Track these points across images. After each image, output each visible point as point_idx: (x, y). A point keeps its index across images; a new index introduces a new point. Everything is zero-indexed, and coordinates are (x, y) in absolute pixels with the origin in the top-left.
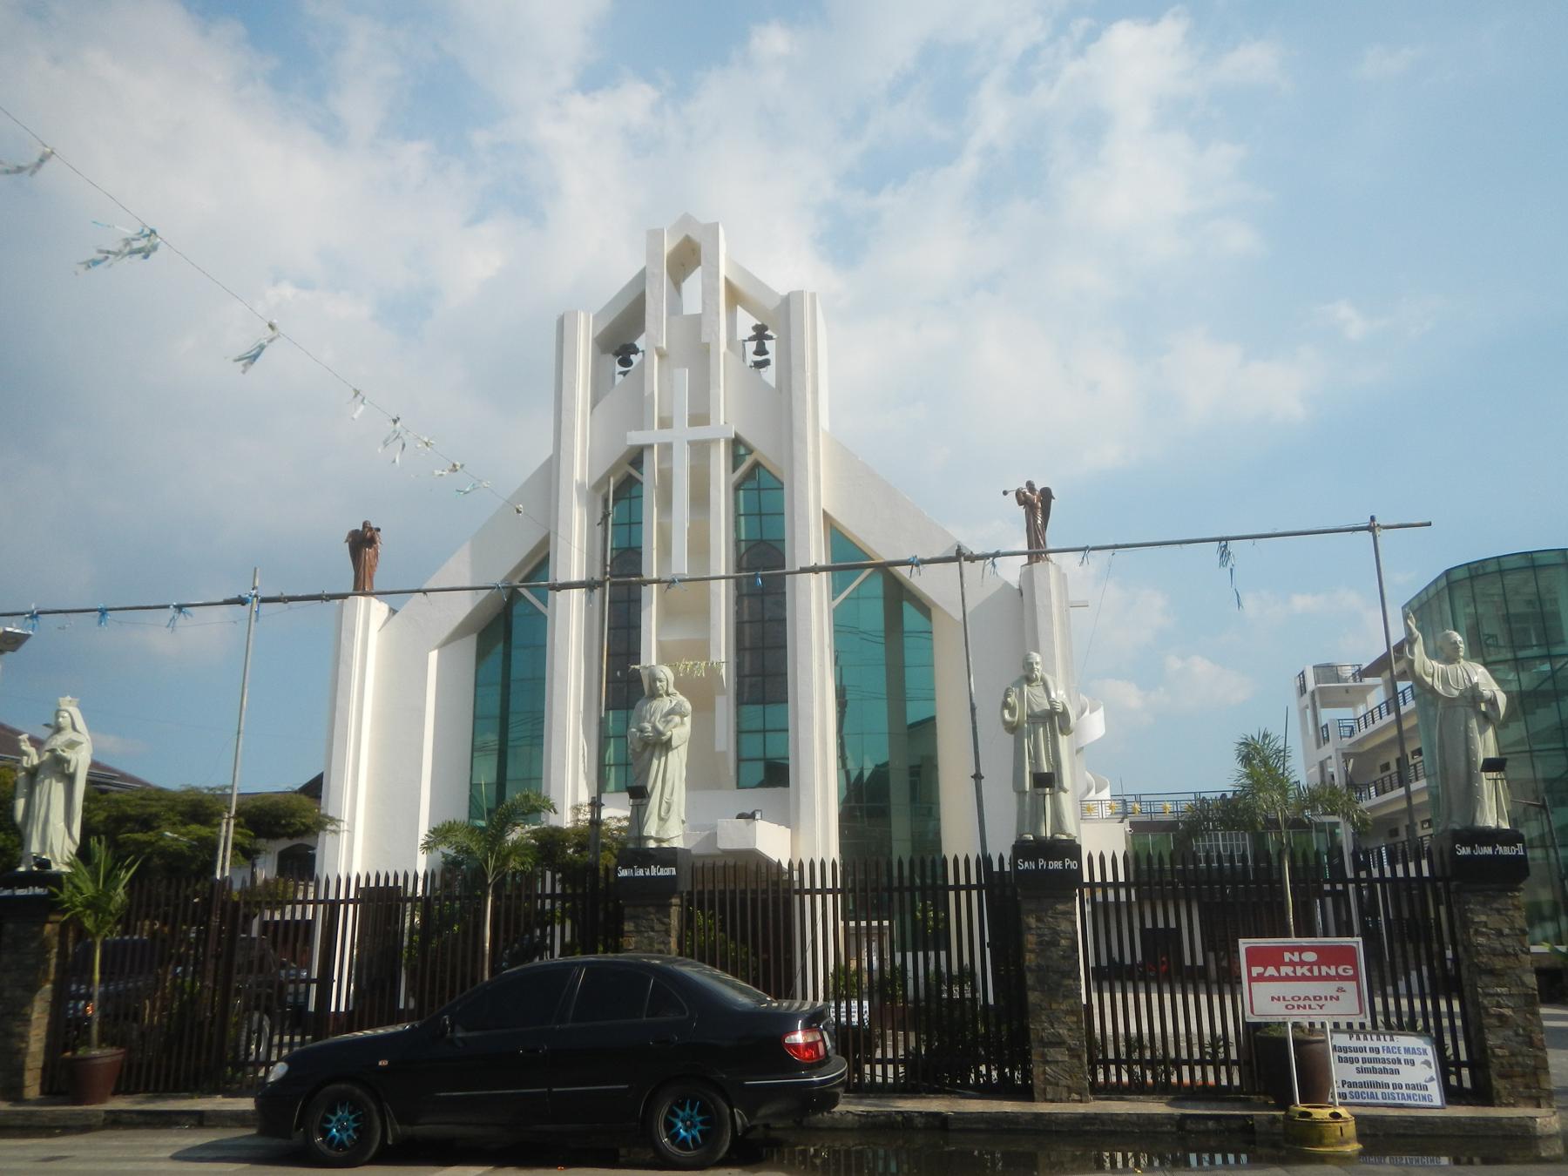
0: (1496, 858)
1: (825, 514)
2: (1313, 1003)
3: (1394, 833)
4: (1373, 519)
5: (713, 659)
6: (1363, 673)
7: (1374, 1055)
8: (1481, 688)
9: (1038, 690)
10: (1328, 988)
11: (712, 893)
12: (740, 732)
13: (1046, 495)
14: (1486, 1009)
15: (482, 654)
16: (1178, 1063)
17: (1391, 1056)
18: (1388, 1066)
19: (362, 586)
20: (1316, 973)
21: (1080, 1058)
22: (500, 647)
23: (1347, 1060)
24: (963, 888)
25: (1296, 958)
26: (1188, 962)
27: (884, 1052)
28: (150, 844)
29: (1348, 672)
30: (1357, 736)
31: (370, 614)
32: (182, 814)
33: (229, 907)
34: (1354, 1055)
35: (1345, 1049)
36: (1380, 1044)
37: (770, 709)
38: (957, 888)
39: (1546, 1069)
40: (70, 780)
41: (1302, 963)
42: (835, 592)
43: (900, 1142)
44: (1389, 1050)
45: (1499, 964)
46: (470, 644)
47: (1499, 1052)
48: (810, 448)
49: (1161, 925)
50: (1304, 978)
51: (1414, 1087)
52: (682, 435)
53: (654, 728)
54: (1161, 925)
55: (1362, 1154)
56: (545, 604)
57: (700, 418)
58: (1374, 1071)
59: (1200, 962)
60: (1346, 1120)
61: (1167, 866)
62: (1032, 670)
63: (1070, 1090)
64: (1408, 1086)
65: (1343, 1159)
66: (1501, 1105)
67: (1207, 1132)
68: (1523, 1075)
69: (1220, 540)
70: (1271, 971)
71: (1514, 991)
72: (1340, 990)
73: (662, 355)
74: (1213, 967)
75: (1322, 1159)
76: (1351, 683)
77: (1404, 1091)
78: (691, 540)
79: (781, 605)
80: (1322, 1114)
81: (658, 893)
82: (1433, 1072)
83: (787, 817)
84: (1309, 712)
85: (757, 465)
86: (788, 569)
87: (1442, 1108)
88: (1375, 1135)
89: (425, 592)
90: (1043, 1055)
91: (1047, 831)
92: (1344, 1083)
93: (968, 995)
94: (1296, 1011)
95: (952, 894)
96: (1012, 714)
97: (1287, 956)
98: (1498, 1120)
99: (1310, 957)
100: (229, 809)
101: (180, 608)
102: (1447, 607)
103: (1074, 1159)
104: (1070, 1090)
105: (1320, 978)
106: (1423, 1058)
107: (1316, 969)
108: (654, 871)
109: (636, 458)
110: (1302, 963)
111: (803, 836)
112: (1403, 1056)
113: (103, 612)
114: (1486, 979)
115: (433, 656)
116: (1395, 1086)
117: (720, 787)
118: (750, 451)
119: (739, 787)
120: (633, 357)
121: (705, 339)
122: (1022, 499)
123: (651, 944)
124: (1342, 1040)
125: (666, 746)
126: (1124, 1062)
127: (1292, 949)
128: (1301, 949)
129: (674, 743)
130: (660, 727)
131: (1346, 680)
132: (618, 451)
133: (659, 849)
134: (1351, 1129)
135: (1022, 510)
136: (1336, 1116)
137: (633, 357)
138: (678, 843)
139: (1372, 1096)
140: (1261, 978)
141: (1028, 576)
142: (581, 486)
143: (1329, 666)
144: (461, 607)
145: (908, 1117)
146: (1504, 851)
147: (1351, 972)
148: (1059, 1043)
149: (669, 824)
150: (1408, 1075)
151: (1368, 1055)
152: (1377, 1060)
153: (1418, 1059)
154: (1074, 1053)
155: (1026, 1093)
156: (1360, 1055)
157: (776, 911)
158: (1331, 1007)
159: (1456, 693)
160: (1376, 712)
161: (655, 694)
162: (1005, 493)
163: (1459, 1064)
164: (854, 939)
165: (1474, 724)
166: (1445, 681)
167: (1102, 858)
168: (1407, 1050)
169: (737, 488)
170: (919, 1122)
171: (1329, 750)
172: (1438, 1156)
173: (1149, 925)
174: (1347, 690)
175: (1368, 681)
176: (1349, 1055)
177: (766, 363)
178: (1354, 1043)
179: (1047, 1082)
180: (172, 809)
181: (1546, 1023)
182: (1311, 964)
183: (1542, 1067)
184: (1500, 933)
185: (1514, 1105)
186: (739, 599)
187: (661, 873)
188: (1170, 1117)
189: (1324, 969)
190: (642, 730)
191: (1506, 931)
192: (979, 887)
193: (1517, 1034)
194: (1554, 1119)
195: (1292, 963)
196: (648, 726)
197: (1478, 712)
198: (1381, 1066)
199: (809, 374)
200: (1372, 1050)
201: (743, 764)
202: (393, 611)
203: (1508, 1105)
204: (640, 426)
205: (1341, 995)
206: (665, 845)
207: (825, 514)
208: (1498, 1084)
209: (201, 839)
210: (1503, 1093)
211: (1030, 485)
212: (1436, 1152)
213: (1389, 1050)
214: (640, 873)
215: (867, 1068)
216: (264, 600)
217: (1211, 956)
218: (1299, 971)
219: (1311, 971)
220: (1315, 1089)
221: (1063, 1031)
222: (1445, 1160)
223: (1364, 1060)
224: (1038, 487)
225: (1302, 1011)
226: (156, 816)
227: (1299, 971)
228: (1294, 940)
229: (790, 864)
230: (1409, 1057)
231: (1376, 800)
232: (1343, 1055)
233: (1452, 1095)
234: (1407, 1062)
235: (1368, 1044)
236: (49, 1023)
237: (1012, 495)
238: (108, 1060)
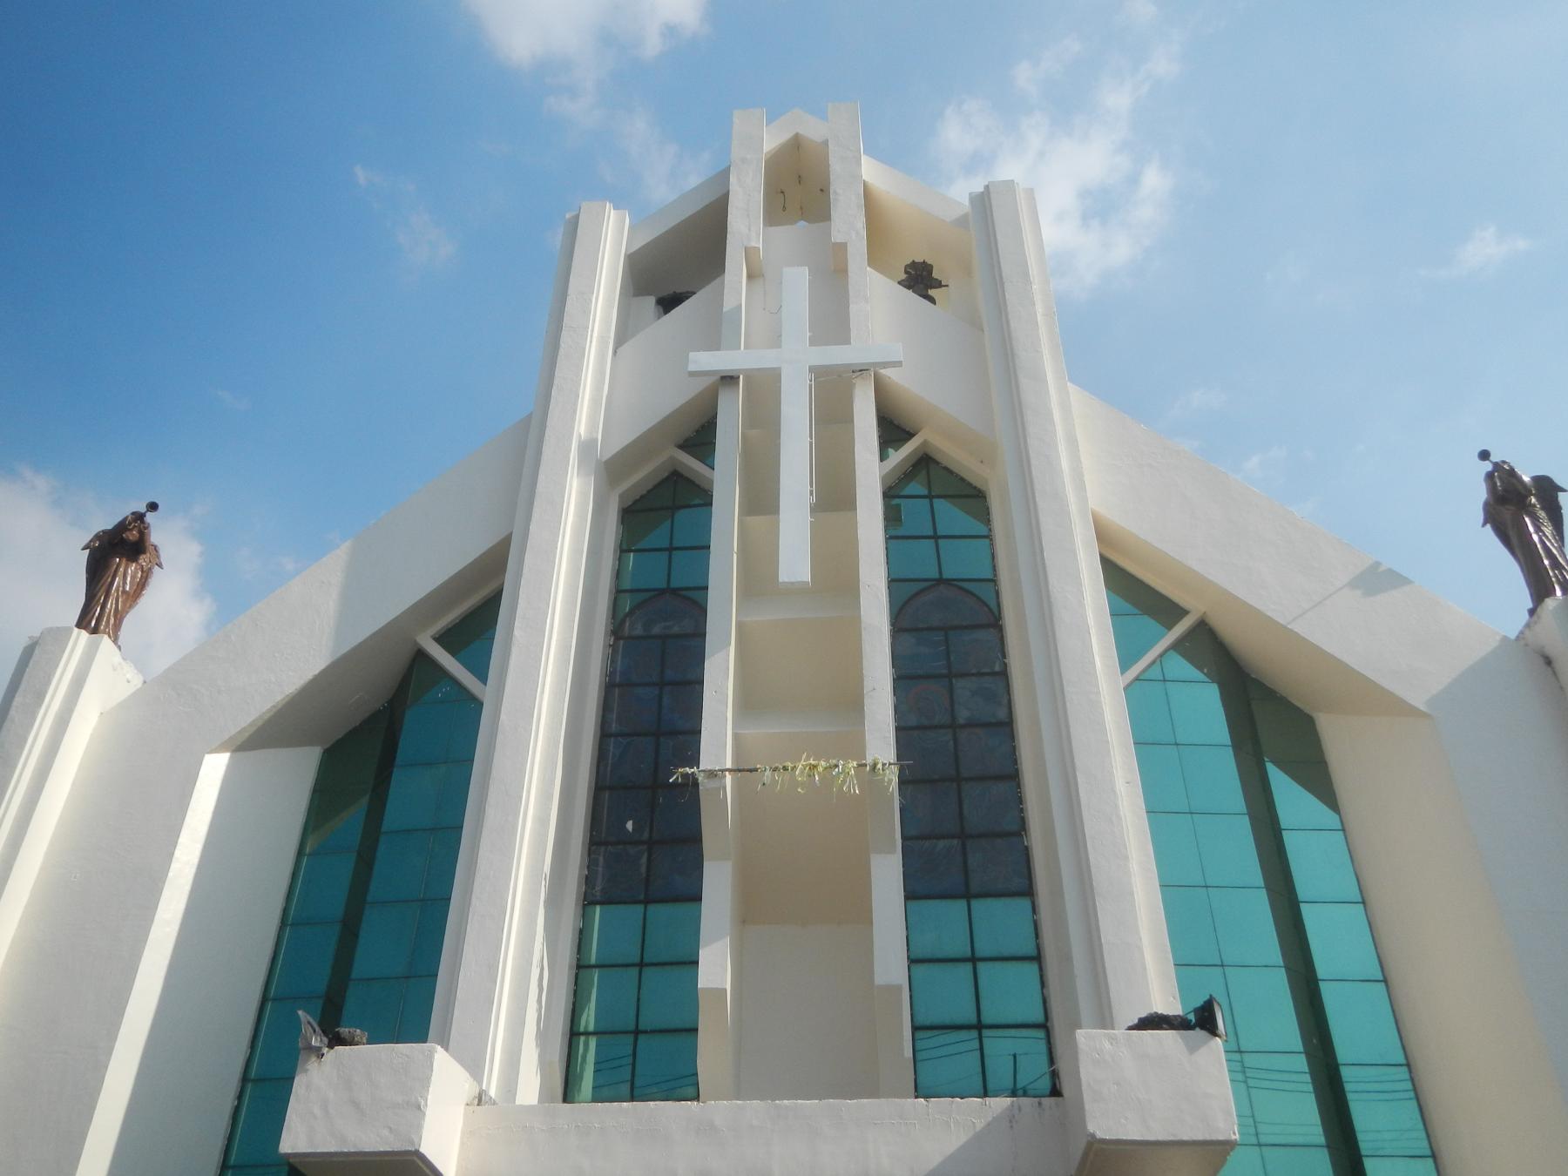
15: (326, 799)
22: (364, 802)
56: (483, 678)
78: (802, 561)
115: (214, 767)
117: (871, 1090)
132: (672, 398)
142: (587, 447)
237: (1488, 466)
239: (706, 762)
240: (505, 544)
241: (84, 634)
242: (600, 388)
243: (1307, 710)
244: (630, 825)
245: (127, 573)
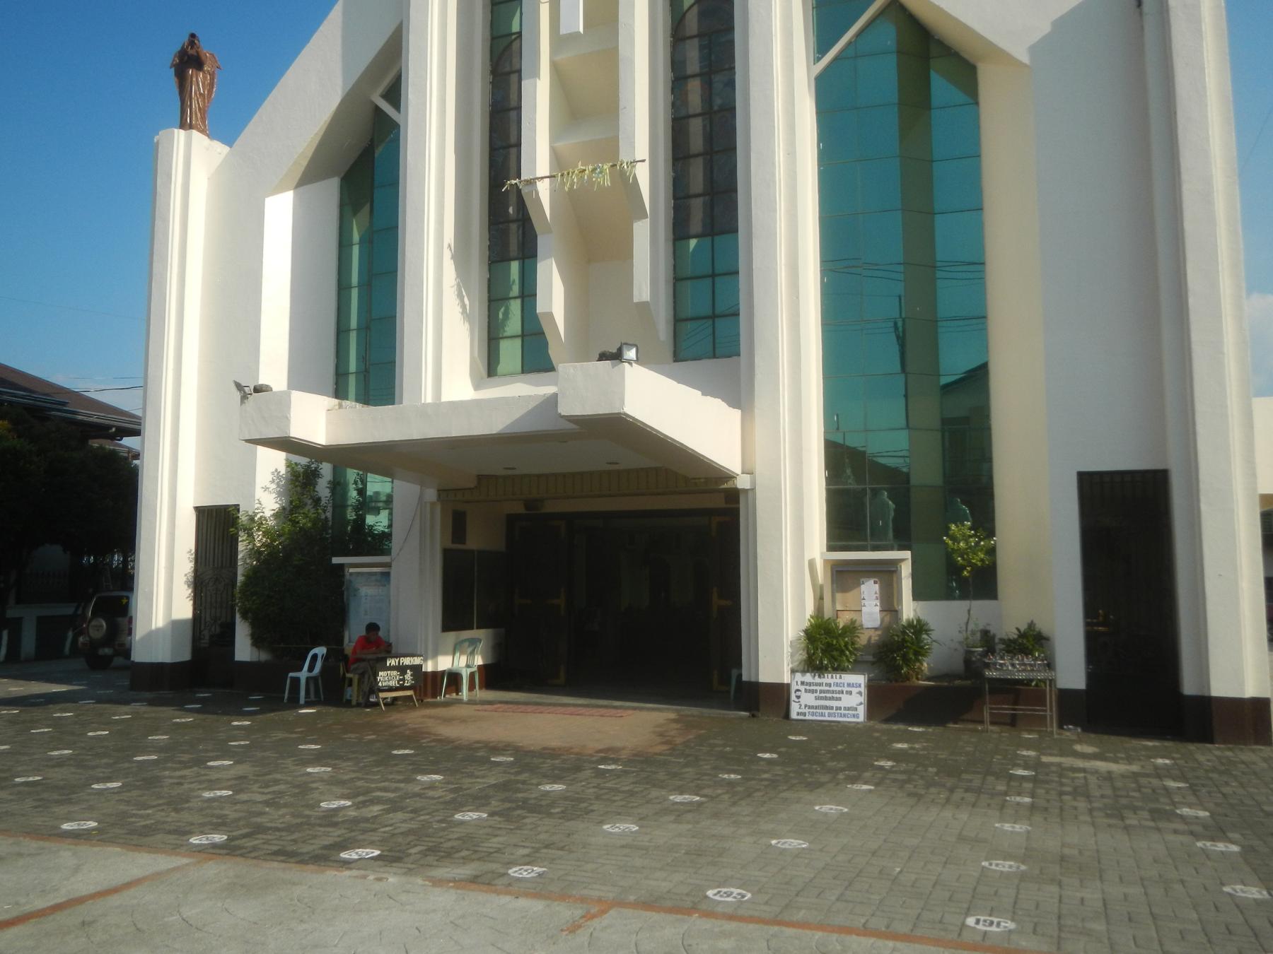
5: (624, 157)
12: (679, 279)
37: (717, 238)
46: (330, 189)
83: (738, 393)
164: (844, 576)
239: (525, 175)
241: (182, 132)
243: (972, 61)
244: (511, 210)
245: (198, 81)
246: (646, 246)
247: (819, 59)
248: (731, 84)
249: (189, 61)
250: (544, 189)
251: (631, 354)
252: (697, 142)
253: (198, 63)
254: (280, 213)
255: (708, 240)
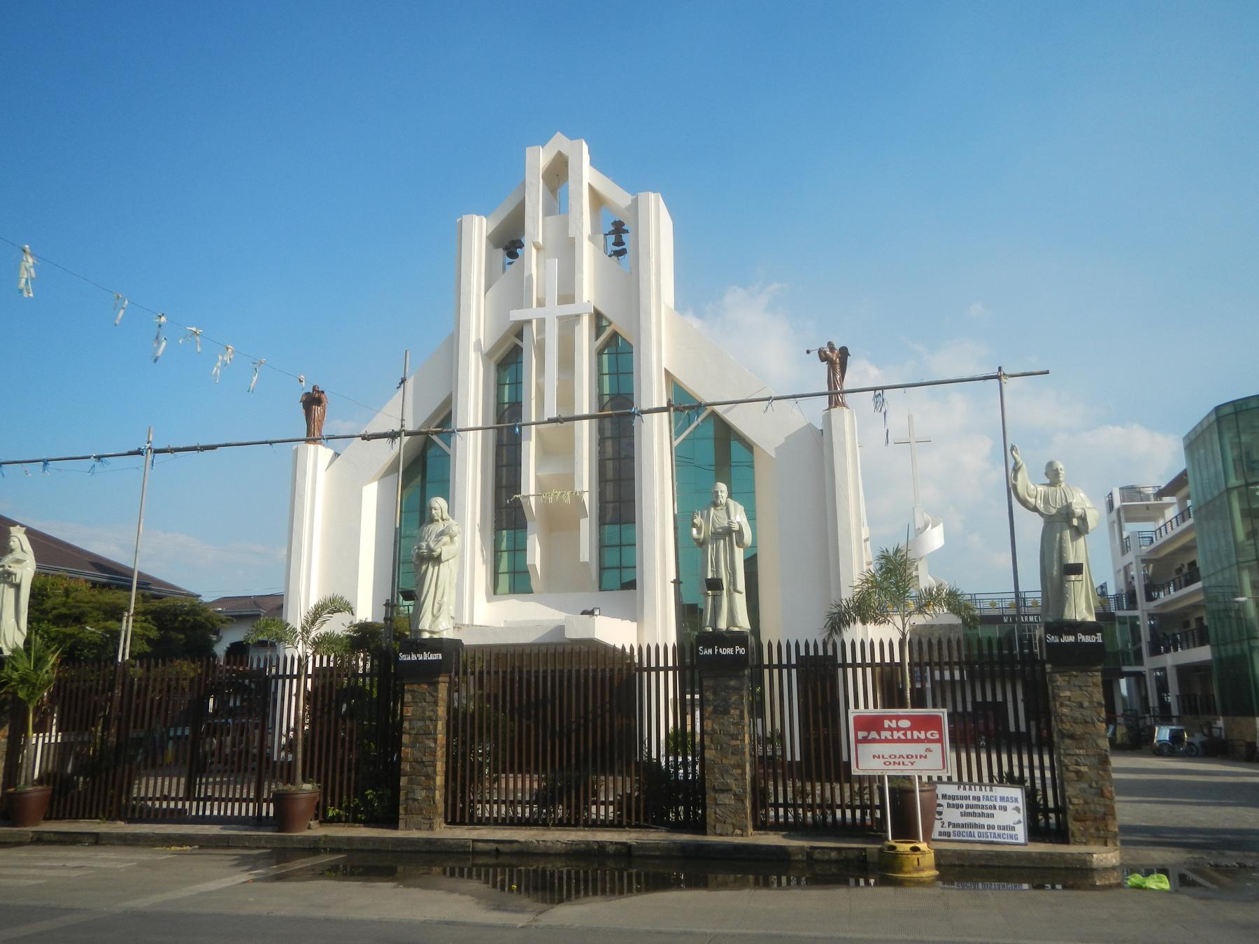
0: (1077, 645)
1: (666, 371)
2: (906, 761)
3: (1187, 624)
4: (1000, 369)
5: (577, 489)
6: (1161, 494)
7: (976, 802)
8: (1074, 506)
9: (722, 513)
10: (919, 749)
11: (562, 672)
12: (602, 546)
13: (844, 353)
14: (1067, 766)
16: (832, 807)
17: (989, 803)
18: (985, 811)
19: (311, 438)
20: (909, 737)
21: (743, 802)
22: (419, 479)
23: (954, 806)
24: (785, 666)
25: (893, 724)
26: (1012, 728)
27: (607, 796)
28: (71, 636)
29: (1150, 491)
30: (1156, 543)
31: (318, 457)
32: (105, 612)
33: (128, 682)
34: (959, 802)
35: (953, 798)
36: (980, 794)
38: (789, 666)
39: (1113, 816)
40: (17, 587)
41: (898, 729)
42: (676, 431)
43: (596, 865)
44: (987, 798)
45: (1079, 730)
47: (1075, 801)
48: (654, 320)
49: (989, 699)
50: (899, 741)
51: (1004, 828)
52: (552, 312)
53: (428, 546)
54: (989, 699)
55: (939, 878)
57: (567, 296)
58: (974, 815)
59: (1023, 728)
60: (924, 853)
61: (995, 652)
62: (717, 497)
63: (734, 827)
64: (999, 827)
65: (920, 883)
66: (1075, 843)
67: (829, 862)
68: (1095, 819)
69: (875, 389)
70: (874, 735)
71: (1091, 752)
72: (928, 750)
73: (538, 249)
74: (1033, 732)
75: (1093, 887)
76: (1152, 502)
77: (996, 831)
79: (631, 445)
80: (904, 847)
81: (428, 673)
82: (1021, 816)
83: (635, 613)
84: (1116, 526)
85: (615, 335)
86: (524, 421)
87: (1025, 844)
88: (962, 866)
89: (271, 443)
90: (715, 799)
91: (723, 625)
92: (949, 824)
93: (779, 753)
94: (892, 767)
95: (766, 672)
96: (699, 532)
97: (887, 723)
98: (1062, 855)
99: (905, 724)
100: (128, 611)
101: (99, 458)
102: (1216, 437)
103: (736, 880)
104: (734, 827)
105: (912, 741)
106: (1014, 805)
107: (909, 733)
108: (426, 656)
109: (518, 331)
110: (898, 729)
111: (644, 629)
112: (998, 804)
113: (46, 462)
114: (1068, 741)
116: (989, 827)
118: (610, 323)
119: (601, 589)
120: (519, 251)
121: (571, 235)
122: (823, 357)
123: (424, 712)
124: (952, 790)
125: (438, 560)
126: (791, 806)
127: (890, 718)
128: (898, 718)
129: (443, 558)
130: (432, 545)
131: (1147, 497)
133: (431, 639)
134: (929, 859)
135: (825, 365)
136: (915, 849)
137: (519, 251)
138: (445, 635)
139: (971, 834)
140: (865, 740)
141: (827, 419)
143: (1132, 488)
144: (387, 452)
145: (601, 845)
146: (1087, 639)
147: (937, 736)
148: (727, 790)
149: (440, 619)
150: (1001, 818)
151: (971, 802)
152: (977, 807)
153: (1010, 806)
154: (739, 798)
155: (699, 826)
156: (964, 802)
157: (561, 685)
158: (920, 763)
159: (1054, 511)
160: (1169, 525)
161: (432, 520)
162: (808, 352)
163: (1046, 811)
165: (1067, 534)
166: (1046, 501)
167: (882, 644)
168: (1002, 799)
169: (600, 353)
170: (611, 849)
171: (1130, 557)
172: (1021, 883)
173: (979, 699)
174: (1148, 507)
175: (1166, 500)
176: (956, 802)
177: (623, 252)
178: (962, 793)
179: (717, 820)
180: (98, 609)
181: (1115, 776)
182: (905, 729)
183: (1109, 813)
184: (1081, 706)
185: (1086, 844)
186: (602, 441)
187: (431, 658)
188: (802, 848)
189: (916, 734)
190: (419, 548)
191: (1086, 704)
192: (674, 669)
193: (1091, 786)
194: (1109, 856)
195: (891, 729)
196: (424, 544)
197: (1071, 526)
198: (980, 811)
199: (653, 260)
200: (974, 798)
201: (606, 574)
202: (337, 455)
203: (1081, 843)
204: (521, 303)
205: (928, 754)
206: (436, 636)
207: (666, 371)
208: (1074, 826)
209: (108, 630)
210: (1076, 833)
211: (831, 345)
212: (1023, 880)
213: (987, 798)
214: (414, 657)
215: (594, 808)
216: (157, 451)
217: (1033, 723)
218: (896, 735)
219: (905, 735)
220: (905, 830)
221: (731, 781)
222: (1025, 886)
223: (968, 806)
224: (837, 347)
225: (897, 767)
226: (83, 614)
227: (896, 735)
228: (909, 711)
229: (632, 648)
230: (1003, 804)
231: (1174, 594)
232: (951, 802)
233: (1036, 832)
234: (1001, 808)
235: (972, 793)
236: (5, 767)
238: (35, 794)
239: (523, 493)
240: (451, 395)
242: (478, 327)
245: (317, 410)
246: (587, 529)
247: (678, 434)
248: (632, 445)
249: (312, 401)
250: (532, 500)
251: (597, 612)
252: (610, 474)
253: (319, 402)
254: (370, 494)
255: (617, 528)
